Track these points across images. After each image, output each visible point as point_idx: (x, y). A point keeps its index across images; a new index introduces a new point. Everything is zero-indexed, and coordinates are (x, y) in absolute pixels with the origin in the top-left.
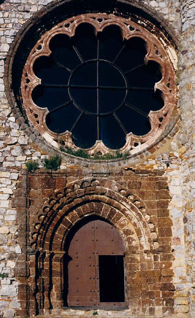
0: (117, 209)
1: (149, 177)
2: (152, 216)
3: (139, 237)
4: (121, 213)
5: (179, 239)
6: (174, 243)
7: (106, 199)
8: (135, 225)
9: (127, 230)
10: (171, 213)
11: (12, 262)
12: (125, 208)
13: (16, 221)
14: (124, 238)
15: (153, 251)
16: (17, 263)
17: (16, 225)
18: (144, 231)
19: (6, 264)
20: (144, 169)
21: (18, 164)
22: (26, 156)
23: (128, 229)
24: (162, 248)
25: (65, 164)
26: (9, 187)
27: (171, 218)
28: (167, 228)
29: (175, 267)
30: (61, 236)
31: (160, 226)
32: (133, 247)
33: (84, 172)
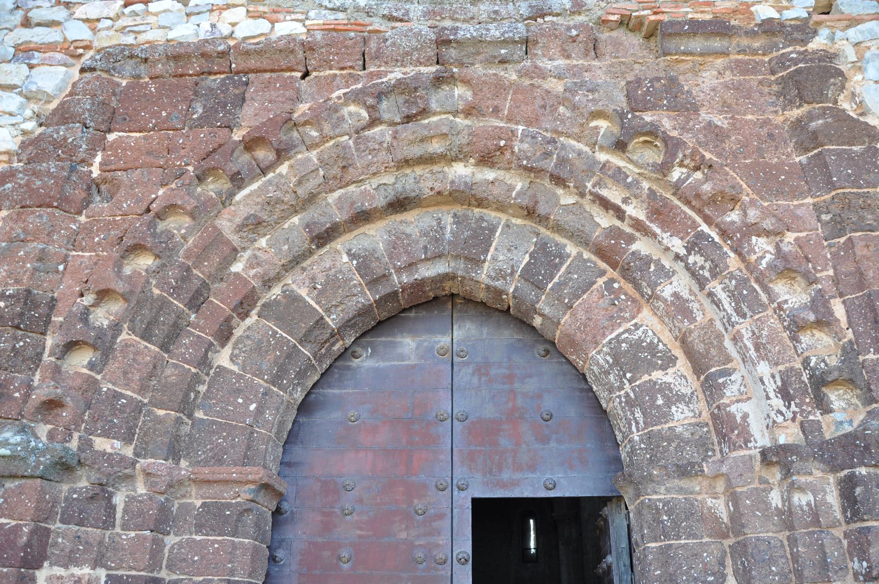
1: (737, 61)
4: (594, 258)
7: (511, 188)
9: (637, 345)
14: (621, 388)
18: (747, 335)
20: (708, 17)
21: (77, 32)
32: (679, 437)
33: (394, 44)
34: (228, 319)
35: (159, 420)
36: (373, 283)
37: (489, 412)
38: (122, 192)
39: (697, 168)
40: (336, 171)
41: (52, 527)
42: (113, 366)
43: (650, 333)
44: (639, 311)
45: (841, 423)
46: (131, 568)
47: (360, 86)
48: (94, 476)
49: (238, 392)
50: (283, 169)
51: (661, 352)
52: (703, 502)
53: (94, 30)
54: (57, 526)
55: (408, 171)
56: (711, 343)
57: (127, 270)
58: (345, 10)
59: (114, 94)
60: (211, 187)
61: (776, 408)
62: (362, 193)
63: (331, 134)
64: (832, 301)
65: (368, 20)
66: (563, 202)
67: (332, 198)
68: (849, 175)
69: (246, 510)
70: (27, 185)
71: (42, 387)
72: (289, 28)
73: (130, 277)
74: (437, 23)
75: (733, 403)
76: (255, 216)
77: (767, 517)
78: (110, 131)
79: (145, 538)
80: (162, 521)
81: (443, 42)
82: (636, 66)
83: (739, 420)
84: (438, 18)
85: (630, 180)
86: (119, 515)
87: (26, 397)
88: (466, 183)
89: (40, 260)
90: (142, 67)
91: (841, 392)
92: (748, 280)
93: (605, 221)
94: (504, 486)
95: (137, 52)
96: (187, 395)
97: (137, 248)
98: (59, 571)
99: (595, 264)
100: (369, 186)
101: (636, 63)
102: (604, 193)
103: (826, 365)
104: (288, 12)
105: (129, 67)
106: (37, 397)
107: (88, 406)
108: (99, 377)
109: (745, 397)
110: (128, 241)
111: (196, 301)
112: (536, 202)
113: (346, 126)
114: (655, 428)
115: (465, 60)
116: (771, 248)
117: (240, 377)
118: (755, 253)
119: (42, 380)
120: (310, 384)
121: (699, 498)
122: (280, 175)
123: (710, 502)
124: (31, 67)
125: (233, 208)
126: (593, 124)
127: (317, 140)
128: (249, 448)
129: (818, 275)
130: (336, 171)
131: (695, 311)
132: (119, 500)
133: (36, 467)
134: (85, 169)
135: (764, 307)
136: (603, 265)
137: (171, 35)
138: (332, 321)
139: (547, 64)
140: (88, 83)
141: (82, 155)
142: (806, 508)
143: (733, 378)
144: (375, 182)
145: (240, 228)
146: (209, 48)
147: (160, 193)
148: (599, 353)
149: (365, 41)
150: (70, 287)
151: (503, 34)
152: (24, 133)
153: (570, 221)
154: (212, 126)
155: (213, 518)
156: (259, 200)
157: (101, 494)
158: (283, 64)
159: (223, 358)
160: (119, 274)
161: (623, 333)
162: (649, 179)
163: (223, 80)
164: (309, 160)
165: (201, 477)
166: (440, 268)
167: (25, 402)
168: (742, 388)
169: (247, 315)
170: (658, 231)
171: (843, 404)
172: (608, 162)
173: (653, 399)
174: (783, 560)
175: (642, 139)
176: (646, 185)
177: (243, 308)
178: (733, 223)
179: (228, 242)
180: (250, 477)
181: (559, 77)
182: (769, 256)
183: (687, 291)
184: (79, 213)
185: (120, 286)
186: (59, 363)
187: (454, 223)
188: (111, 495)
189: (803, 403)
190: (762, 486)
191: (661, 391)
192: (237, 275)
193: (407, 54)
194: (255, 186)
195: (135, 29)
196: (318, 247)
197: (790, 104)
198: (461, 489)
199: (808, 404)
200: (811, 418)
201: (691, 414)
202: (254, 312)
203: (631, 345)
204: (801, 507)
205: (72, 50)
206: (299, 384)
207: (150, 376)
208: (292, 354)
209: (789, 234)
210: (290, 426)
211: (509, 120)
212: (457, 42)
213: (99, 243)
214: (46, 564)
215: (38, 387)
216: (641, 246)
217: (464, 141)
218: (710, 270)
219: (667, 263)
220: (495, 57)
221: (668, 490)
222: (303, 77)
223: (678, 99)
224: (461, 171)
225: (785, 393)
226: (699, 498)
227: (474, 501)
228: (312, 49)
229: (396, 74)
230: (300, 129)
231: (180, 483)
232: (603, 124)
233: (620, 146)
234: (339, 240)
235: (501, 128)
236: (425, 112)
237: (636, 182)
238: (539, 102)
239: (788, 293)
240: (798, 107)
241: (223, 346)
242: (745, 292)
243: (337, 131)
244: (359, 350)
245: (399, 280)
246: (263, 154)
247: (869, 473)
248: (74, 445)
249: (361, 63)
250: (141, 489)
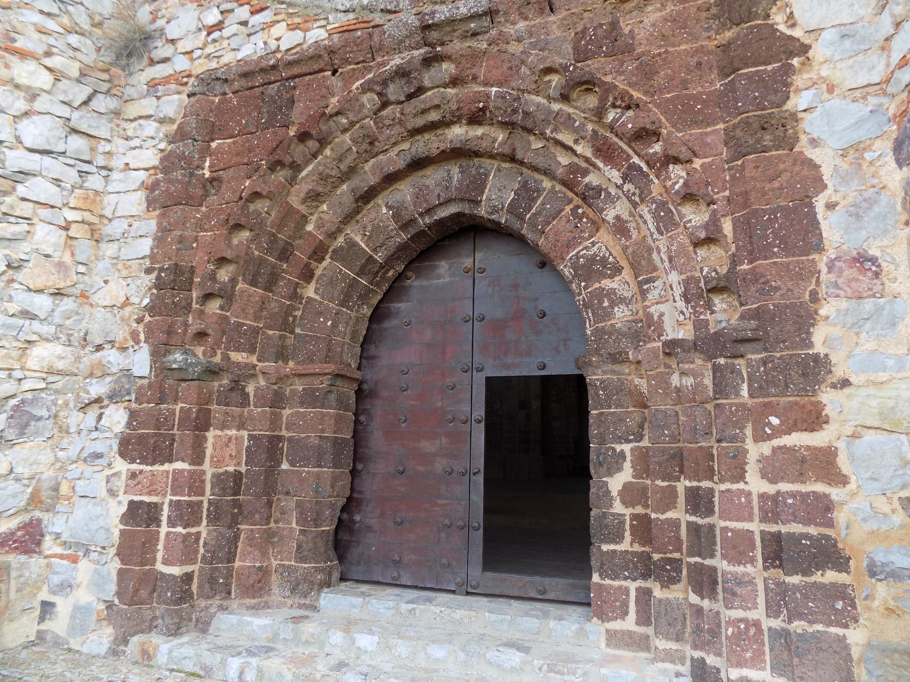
0: (545, 174)
2: (697, 163)
3: (640, 284)
4: (564, 189)
5: (873, 260)
6: (836, 286)
8: (620, 228)
9: (592, 260)
10: (811, 125)
11: (117, 410)
12: (576, 160)
13: (153, 257)
14: (580, 294)
15: (710, 344)
16: (133, 415)
17: (148, 271)
18: (663, 249)
19: (100, 417)
21: (181, 64)
22: (204, 33)
23: (595, 255)
24: (753, 323)
25: (323, 23)
26: (151, 143)
27: (813, 154)
28: (781, 209)
29: (855, 436)
30: (331, 305)
31: (745, 205)
32: (619, 332)
33: (390, 35)
34: (307, 265)
35: (269, 338)
36: (404, 227)
37: (499, 313)
38: (224, 187)
39: (628, 107)
40: (365, 146)
41: (212, 408)
42: (235, 306)
43: (604, 248)
44: (597, 230)
45: (721, 322)
46: (261, 430)
47: (370, 76)
48: (230, 377)
49: (320, 313)
50: (328, 152)
51: (610, 264)
52: (632, 381)
53: (192, 60)
54: (214, 407)
55: (419, 137)
56: (643, 256)
57: (235, 241)
58: (354, 11)
59: (211, 111)
60: (281, 173)
61: (679, 309)
62: (388, 159)
63: (355, 119)
64: (722, 220)
65: (371, 17)
66: (533, 147)
67: (367, 167)
68: (756, 98)
69: (330, 392)
70: (167, 189)
71: (194, 324)
72: (317, 34)
73: (237, 245)
74: (421, 9)
75: (653, 304)
76: (313, 190)
77: (666, 394)
78: (213, 140)
79: (266, 412)
80: (277, 401)
81: (426, 28)
82: (586, 15)
83: (656, 318)
84: (421, 4)
85: (577, 124)
86: (251, 399)
87: (185, 331)
88: (461, 141)
89: (180, 242)
90: (225, 86)
91: (725, 296)
92: (667, 202)
93: (564, 159)
94: (508, 367)
95: (219, 75)
96: (285, 320)
97: (238, 227)
98: (219, 432)
99: (565, 194)
100: (393, 153)
101: (585, 11)
102: (560, 137)
103: (717, 273)
104: (315, 20)
105: (218, 87)
106: (191, 330)
107: (224, 333)
108: (228, 314)
109: (664, 299)
110: (232, 223)
111: (285, 254)
112: (514, 150)
113: (365, 111)
114: (600, 325)
115: (446, 39)
116: (684, 174)
117: (321, 303)
118: (670, 179)
119: (194, 318)
120: (375, 301)
121: (630, 378)
122: (326, 157)
123: (637, 381)
124: (158, 98)
125: (298, 186)
126: (547, 78)
127: (347, 126)
128: (329, 350)
129: (715, 197)
130: (365, 146)
131: (632, 229)
132: (250, 389)
133: (193, 374)
134: (201, 172)
135: (677, 225)
136: (571, 195)
137: (240, 55)
138: (379, 257)
139: (510, 30)
140: (192, 106)
141: (196, 163)
142: (690, 388)
143: (655, 285)
144: (396, 150)
145: (304, 201)
146: (264, 64)
147: (247, 184)
148: (565, 266)
149: (370, 35)
150: (202, 258)
151: (469, 11)
152: (162, 151)
153: (540, 162)
154: (274, 126)
155: (310, 398)
156: (314, 178)
157: (237, 386)
158: (316, 67)
159: (310, 291)
160: (229, 246)
161: (582, 250)
162: (591, 121)
163: (279, 87)
164: (343, 142)
165: (298, 372)
166: (452, 209)
167: (185, 335)
168: (663, 293)
169: (323, 259)
170: (601, 165)
171: (725, 306)
172: (561, 110)
173: (601, 302)
174: (675, 426)
175: (584, 87)
176: (590, 127)
177: (318, 253)
178: (656, 153)
179: (298, 211)
180: (326, 371)
181: (519, 40)
182: (681, 181)
183: (627, 214)
184: (201, 205)
185: (229, 254)
186: (202, 308)
187: (460, 172)
188: (244, 387)
189: (697, 305)
190: (667, 370)
191: (608, 295)
192: (310, 232)
193: (401, 42)
194: (310, 168)
195: (217, 54)
196: (365, 204)
197: (723, 27)
198: (479, 370)
199: (701, 306)
200: (702, 317)
201: (630, 313)
202: (328, 257)
203: (587, 260)
204: (687, 386)
205: (180, 79)
206: (363, 304)
207: (262, 309)
208: (353, 284)
209: (695, 159)
210: (365, 332)
211: (486, 84)
212: (434, 25)
213: (214, 225)
214: (211, 429)
215: (192, 324)
216: (592, 179)
217: (454, 107)
218: (640, 196)
219: (613, 191)
220: (467, 32)
221: (604, 373)
222: (333, 74)
223: (616, 43)
224: (458, 132)
225: (686, 297)
226: (630, 378)
227: (488, 379)
228: (332, 52)
229: (397, 61)
230: (335, 119)
231: (287, 376)
232: (555, 79)
233: (565, 98)
234: (380, 196)
235: (480, 92)
236: (421, 90)
237: (583, 125)
238: (506, 65)
239: (694, 212)
240: (729, 29)
241: (309, 282)
242: (662, 214)
243: (360, 116)
244: (410, 274)
245: (423, 222)
246: (312, 144)
247: (726, 363)
248: (218, 359)
249: (370, 55)
250: (263, 383)
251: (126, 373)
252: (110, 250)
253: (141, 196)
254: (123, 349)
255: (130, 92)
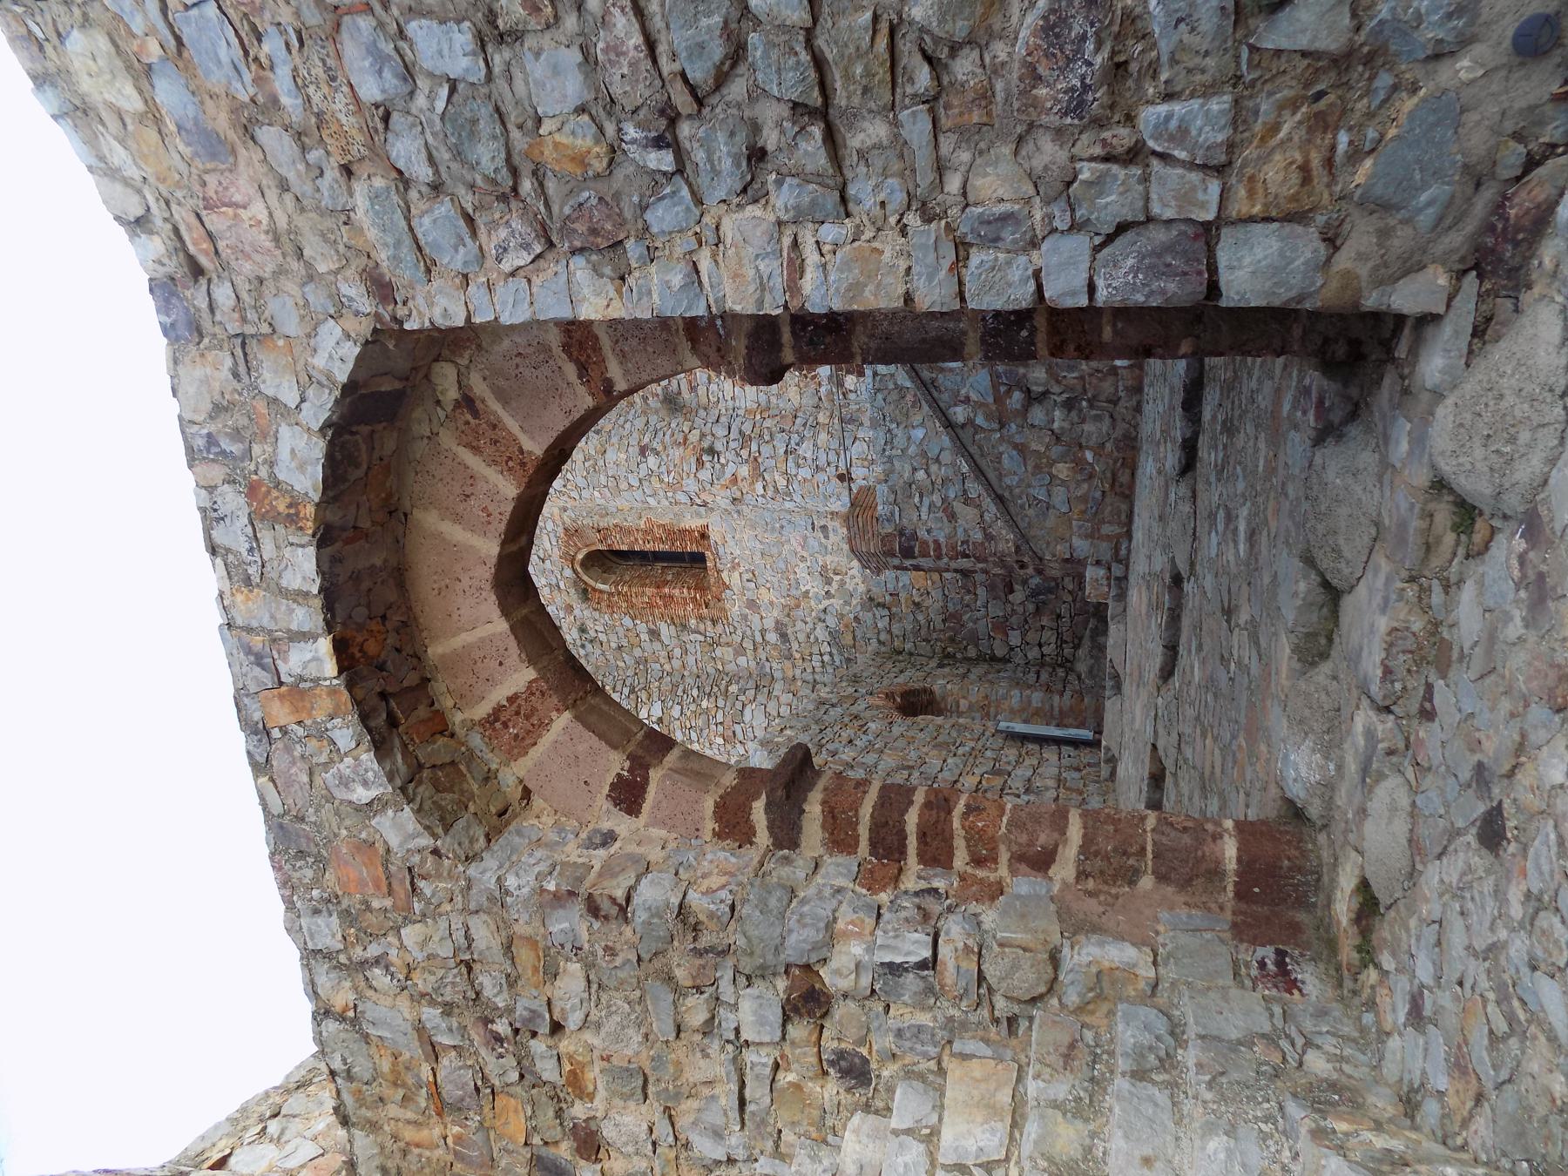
16: (848, 372)
251: (830, 378)
252: (774, 400)
253: (748, 387)
254: (820, 384)
255: (694, 405)
